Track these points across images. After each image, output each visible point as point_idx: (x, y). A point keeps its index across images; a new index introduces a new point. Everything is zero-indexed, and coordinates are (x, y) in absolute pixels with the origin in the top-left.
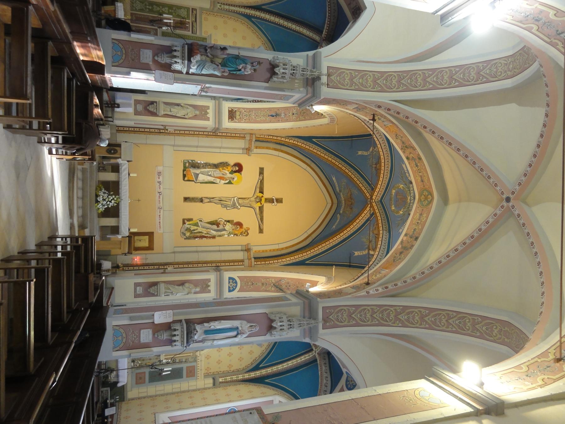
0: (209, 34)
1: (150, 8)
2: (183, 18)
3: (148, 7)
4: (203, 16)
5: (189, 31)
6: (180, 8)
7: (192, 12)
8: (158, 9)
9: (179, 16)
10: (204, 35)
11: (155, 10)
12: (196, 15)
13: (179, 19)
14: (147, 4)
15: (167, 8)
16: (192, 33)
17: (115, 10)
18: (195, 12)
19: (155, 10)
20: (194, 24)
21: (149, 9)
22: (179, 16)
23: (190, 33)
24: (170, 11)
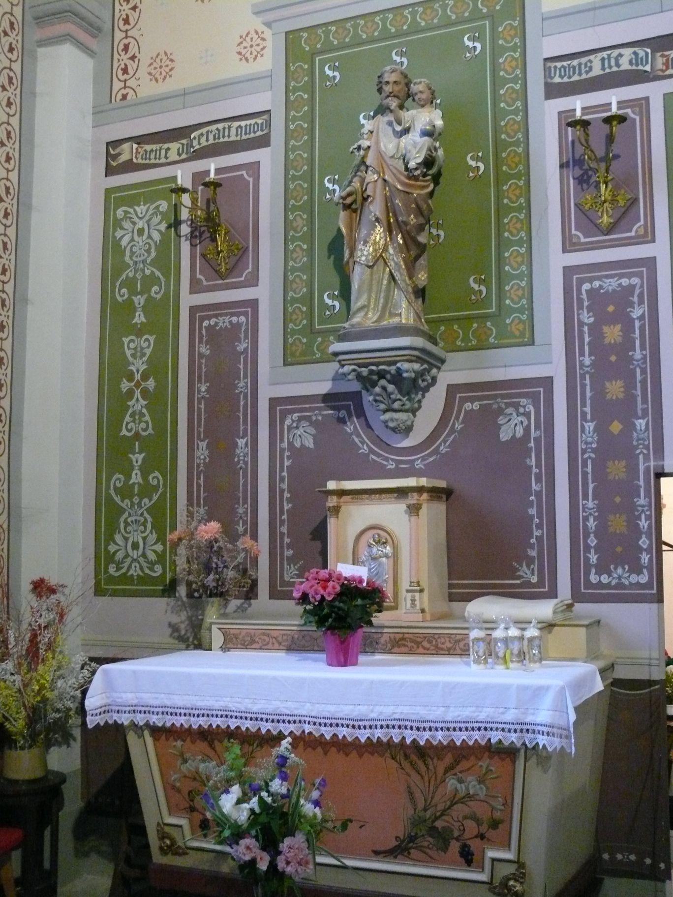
0: (257, 23)
1: (138, 458)
2: (176, 224)
3: (136, 477)
4: (146, 88)
5: (254, 168)
6: (112, 255)
7: (130, 167)
8: (138, 403)
9: (165, 258)
10: (270, 59)
11: (146, 426)
12: (140, 140)
13: (185, 247)
14: (118, 479)
15: (129, 344)
16: (263, 142)
17: (157, 732)
18: (126, 152)
19: (146, 426)
20: (200, 140)
21: (145, 472)
22: (165, 258)
23: (269, 161)
24: (139, 318)
